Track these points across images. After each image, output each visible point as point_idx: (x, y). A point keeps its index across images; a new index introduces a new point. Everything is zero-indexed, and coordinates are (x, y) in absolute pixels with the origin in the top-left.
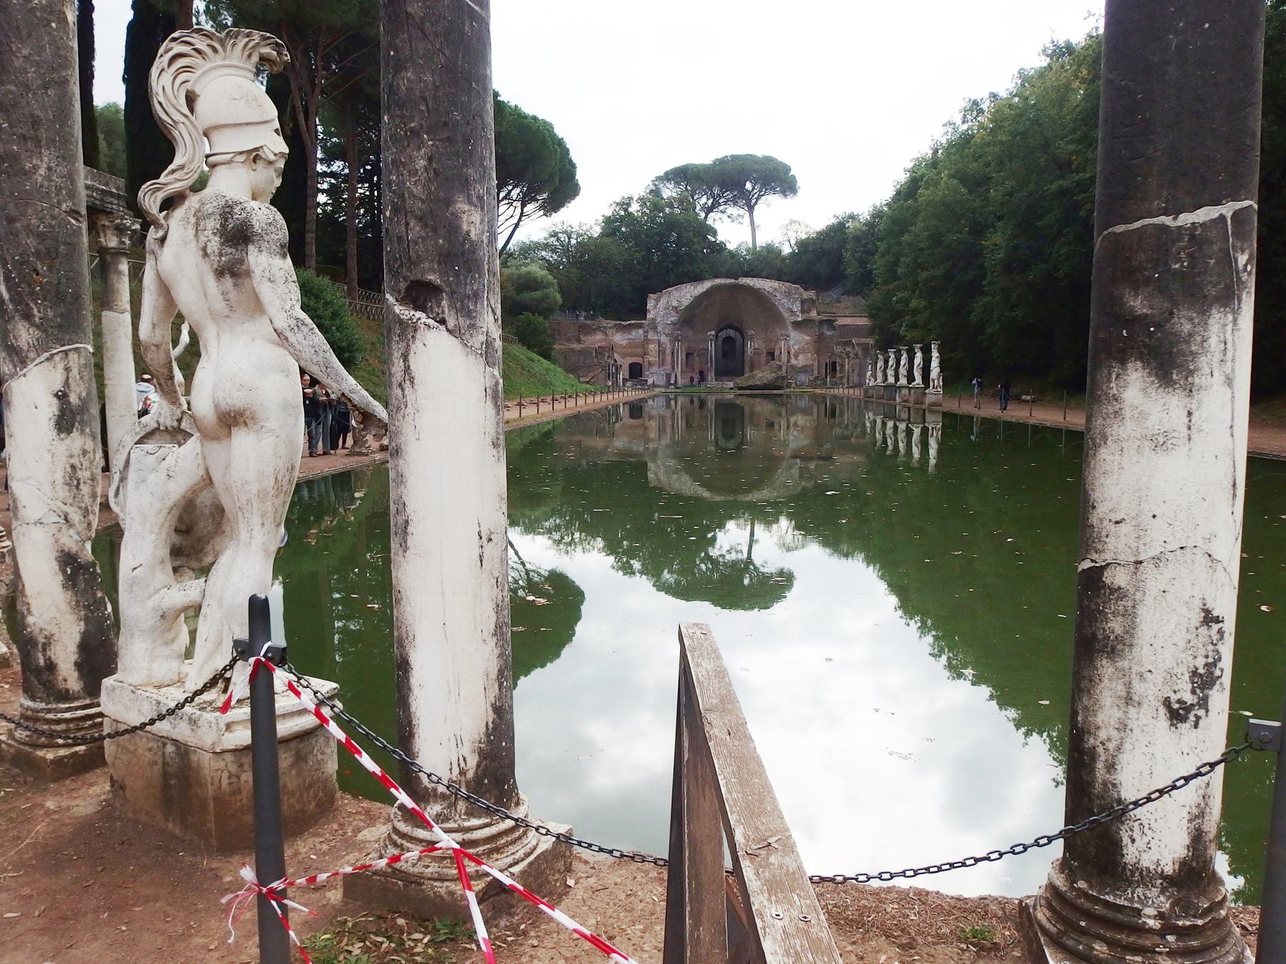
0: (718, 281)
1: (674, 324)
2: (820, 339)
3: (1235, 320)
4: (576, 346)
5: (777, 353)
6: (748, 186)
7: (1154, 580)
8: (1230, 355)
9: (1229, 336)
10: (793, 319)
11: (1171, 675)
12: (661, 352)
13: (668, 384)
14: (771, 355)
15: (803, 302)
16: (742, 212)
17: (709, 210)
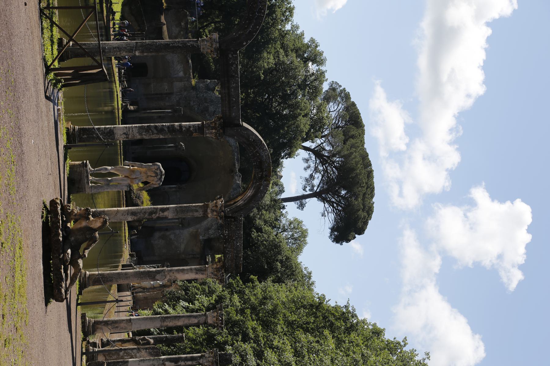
6: (343, 192)
17: (317, 153)
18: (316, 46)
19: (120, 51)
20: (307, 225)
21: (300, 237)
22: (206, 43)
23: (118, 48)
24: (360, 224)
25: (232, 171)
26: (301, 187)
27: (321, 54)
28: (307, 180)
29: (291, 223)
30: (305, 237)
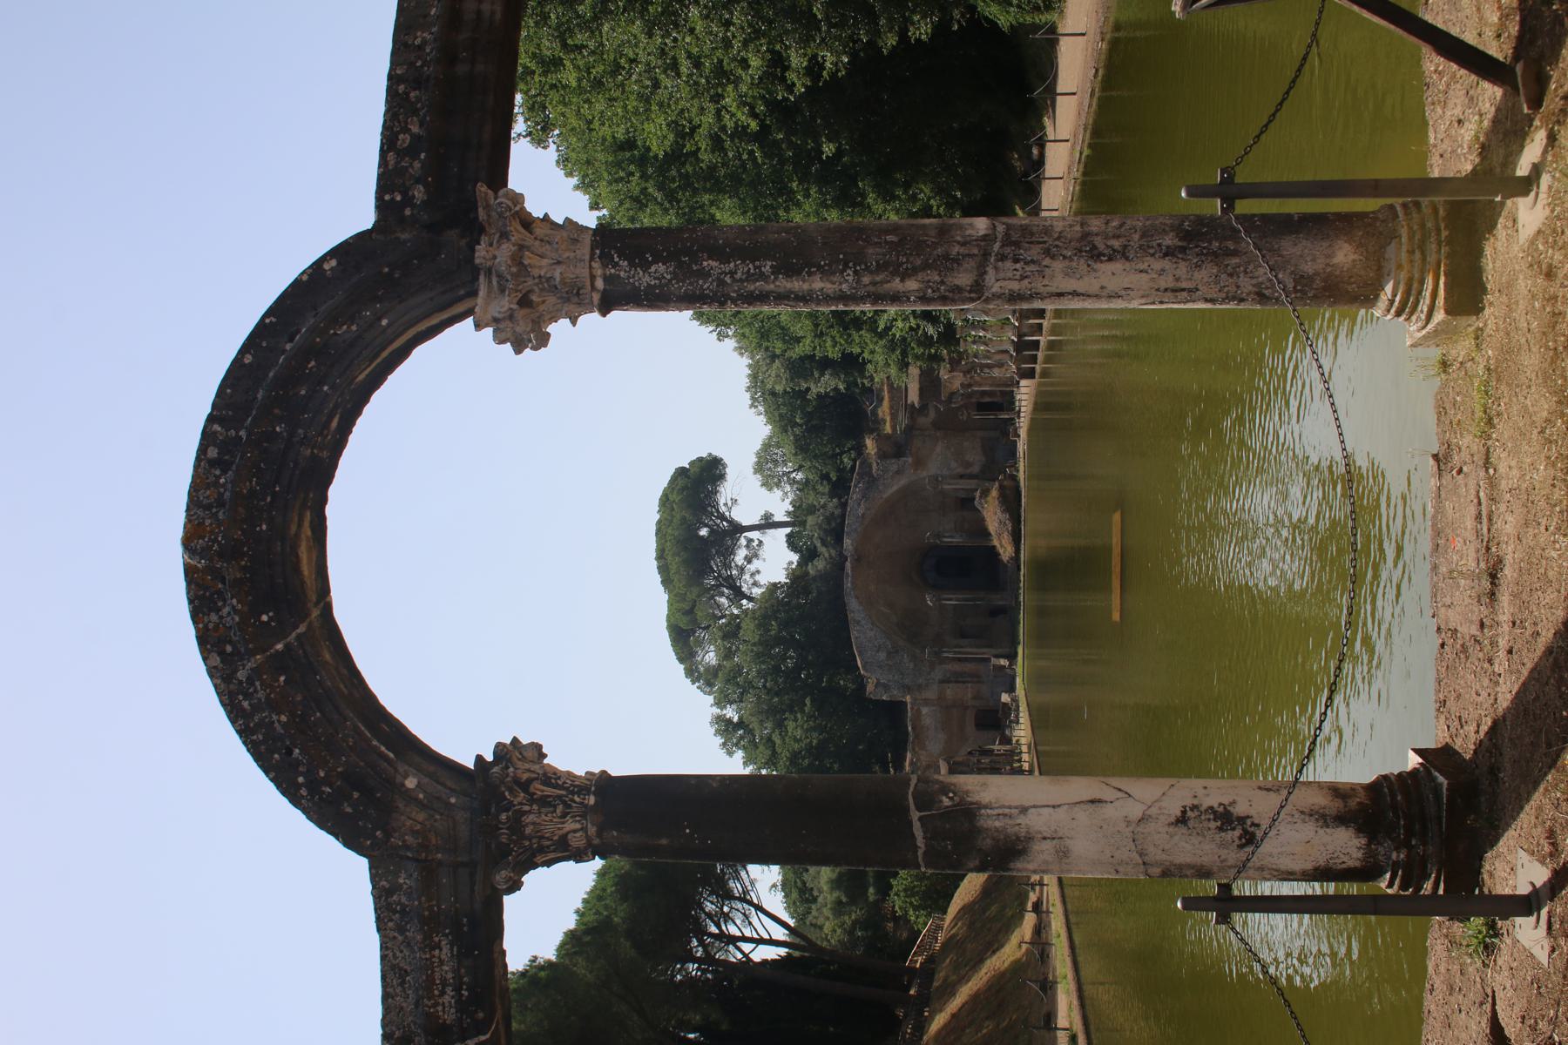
3: (986, 807)
5: (963, 495)
6: (704, 532)
7: (1155, 854)
8: (1007, 811)
9: (995, 812)
11: (1222, 845)
12: (958, 678)
16: (743, 542)
17: (738, 594)
18: (724, 744)
19: (1086, 236)
20: (756, 480)
21: (765, 466)
22: (557, 273)
23: (1095, 255)
24: (681, 482)
25: (858, 560)
26: (766, 547)
27: (718, 732)
28: (756, 556)
29: (778, 485)
30: (758, 463)
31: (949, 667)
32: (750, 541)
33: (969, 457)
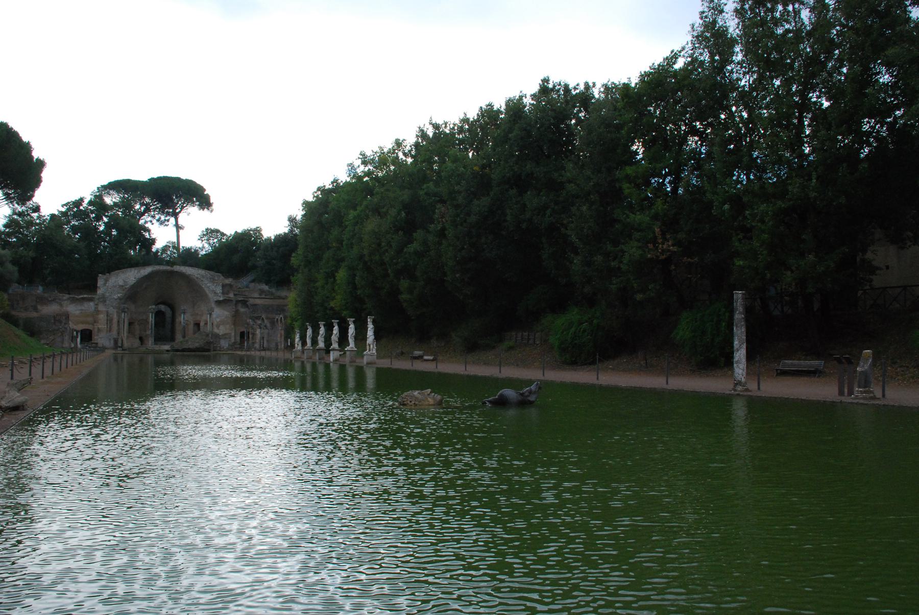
0: (157, 268)
1: (120, 299)
2: (236, 315)
4: (35, 314)
5: (202, 324)
10: (216, 298)
12: (109, 321)
13: (116, 346)
14: (197, 325)
15: (223, 286)
31: (115, 316)
32: (168, 221)
33: (221, 327)
